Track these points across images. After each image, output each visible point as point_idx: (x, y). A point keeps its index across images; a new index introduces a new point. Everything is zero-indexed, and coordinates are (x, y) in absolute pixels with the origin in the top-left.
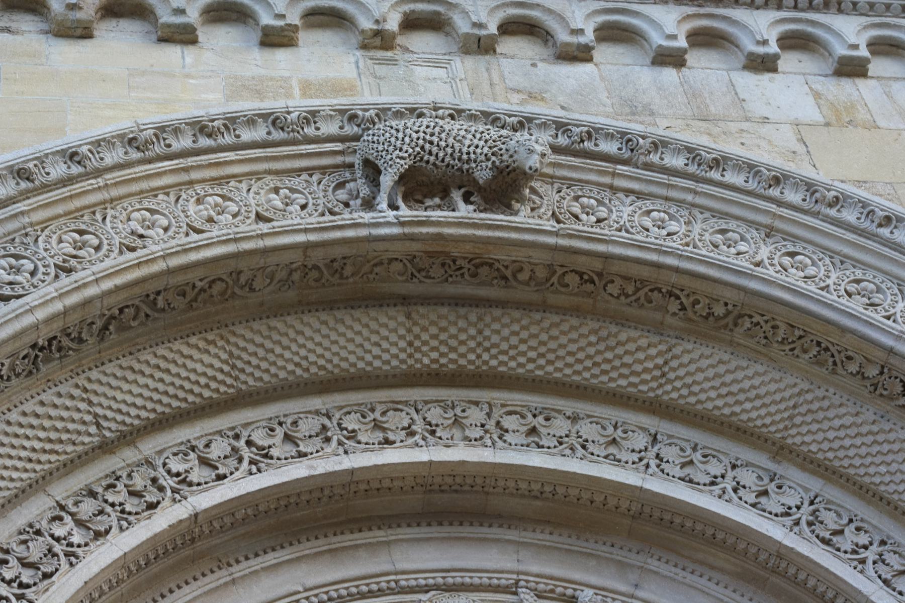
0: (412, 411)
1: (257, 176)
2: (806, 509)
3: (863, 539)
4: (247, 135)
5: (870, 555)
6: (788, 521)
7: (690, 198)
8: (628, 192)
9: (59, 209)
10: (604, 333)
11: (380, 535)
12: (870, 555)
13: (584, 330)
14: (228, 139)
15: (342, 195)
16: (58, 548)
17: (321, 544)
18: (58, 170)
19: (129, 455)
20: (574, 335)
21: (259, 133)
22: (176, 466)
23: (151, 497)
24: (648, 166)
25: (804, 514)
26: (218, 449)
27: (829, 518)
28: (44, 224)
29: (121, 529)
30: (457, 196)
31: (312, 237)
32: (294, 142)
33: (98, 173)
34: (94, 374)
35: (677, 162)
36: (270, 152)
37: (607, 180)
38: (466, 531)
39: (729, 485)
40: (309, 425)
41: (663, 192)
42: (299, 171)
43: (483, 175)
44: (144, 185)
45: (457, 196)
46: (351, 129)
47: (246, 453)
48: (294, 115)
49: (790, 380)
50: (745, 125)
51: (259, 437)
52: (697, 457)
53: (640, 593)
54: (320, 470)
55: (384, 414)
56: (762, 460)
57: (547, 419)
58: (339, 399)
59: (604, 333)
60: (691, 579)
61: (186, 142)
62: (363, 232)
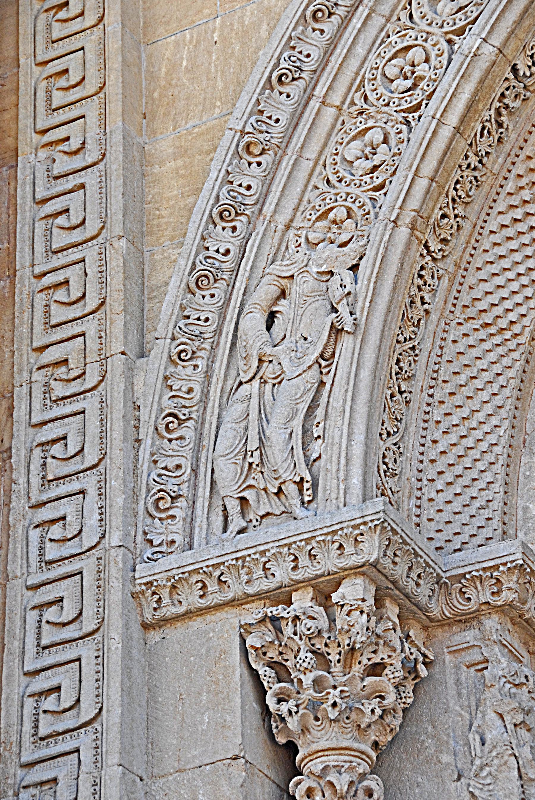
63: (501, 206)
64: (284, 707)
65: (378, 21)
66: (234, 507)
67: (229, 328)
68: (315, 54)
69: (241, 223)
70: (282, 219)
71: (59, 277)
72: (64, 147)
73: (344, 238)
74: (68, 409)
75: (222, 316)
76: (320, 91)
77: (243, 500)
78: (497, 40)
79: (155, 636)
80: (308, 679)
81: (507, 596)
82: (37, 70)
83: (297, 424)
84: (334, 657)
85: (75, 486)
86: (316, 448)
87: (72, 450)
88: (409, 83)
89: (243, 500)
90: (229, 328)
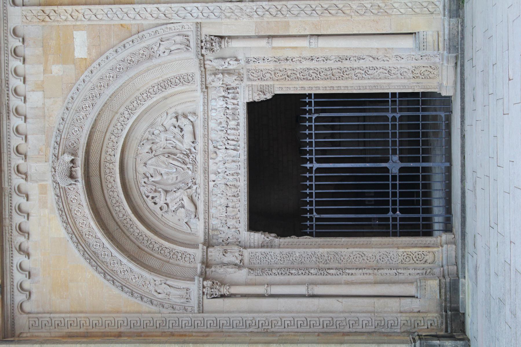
0: (106, 176)
1: (68, 204)
2: (128, 110)
3: (136, 102)
4: (61, 206)
5: (139, 102)
6: (132, 115)
7: (69, 125)
8: (67, 136)
9: (82, 238)
10: (94, 142)
11: (127, 181)
12: (139, 102)
13: (94, 145)
14: (63, 209)
15: (72, 189)
16: (140, 234)
17: (129, 191)
18: (75, 239)
19: (120, 223)
20: (94, 147)
21: (61, 204)
22: (121, 215)
23: (128, 220)
24: (62, 131)
25: (130, 111)
26: (117, 208)
27: (130, 107)
28: (85, 241)
29: (136, 224)
30: (73, 169)
31: (86, 196)
32: (61, 197)
33: (73, 232)
34: (110, 230)
35: (62, 126)
36: (64, 202)
37: (65, 140)
38: (125, 166)
39: (123, 123)
40: (111, 193)
41: (68, 129)
42: (66, 196)
43: (72, 165)
44: (74, 224)
45: (73, 169)
46: (58, 187)
47: (118, 204)
48: (57, 198)
49: (106, 111)
50: (46, 109)
51: (114, 201)
52: (116, 127)
53: (138, 138)
54: (122, 193)
55: (107, 181)
56: (117, 116)
57: (107, 152)
58: (104, 188)
59: (94, 142)
60: (136, 128)
61: (65, 217)
62: (84, 187)
63: (145, 262)
64: (218, 294)
65: (115, 275)
66: (187, 300)
67: (159, 300)
68: (119, 284)
69: (143, 297)
70: (143, 291)
71: (145, 324)
72: (122, 324)
73: (148, 282)
74: (168, 323)
75: (156, 301)
76: (124, 284)
77: (187, 299)
78: (126, 257)
79: (204, 311)
80: (215, 290)
81: (204, 267)
82: (106, 329)
83: (178, 290)
84: (212, 287)
85: (181, 322)
86: (182, 287)
87: (175, 322)
88: (126, 272)
89: (187, 299)
90: (159, 300)
